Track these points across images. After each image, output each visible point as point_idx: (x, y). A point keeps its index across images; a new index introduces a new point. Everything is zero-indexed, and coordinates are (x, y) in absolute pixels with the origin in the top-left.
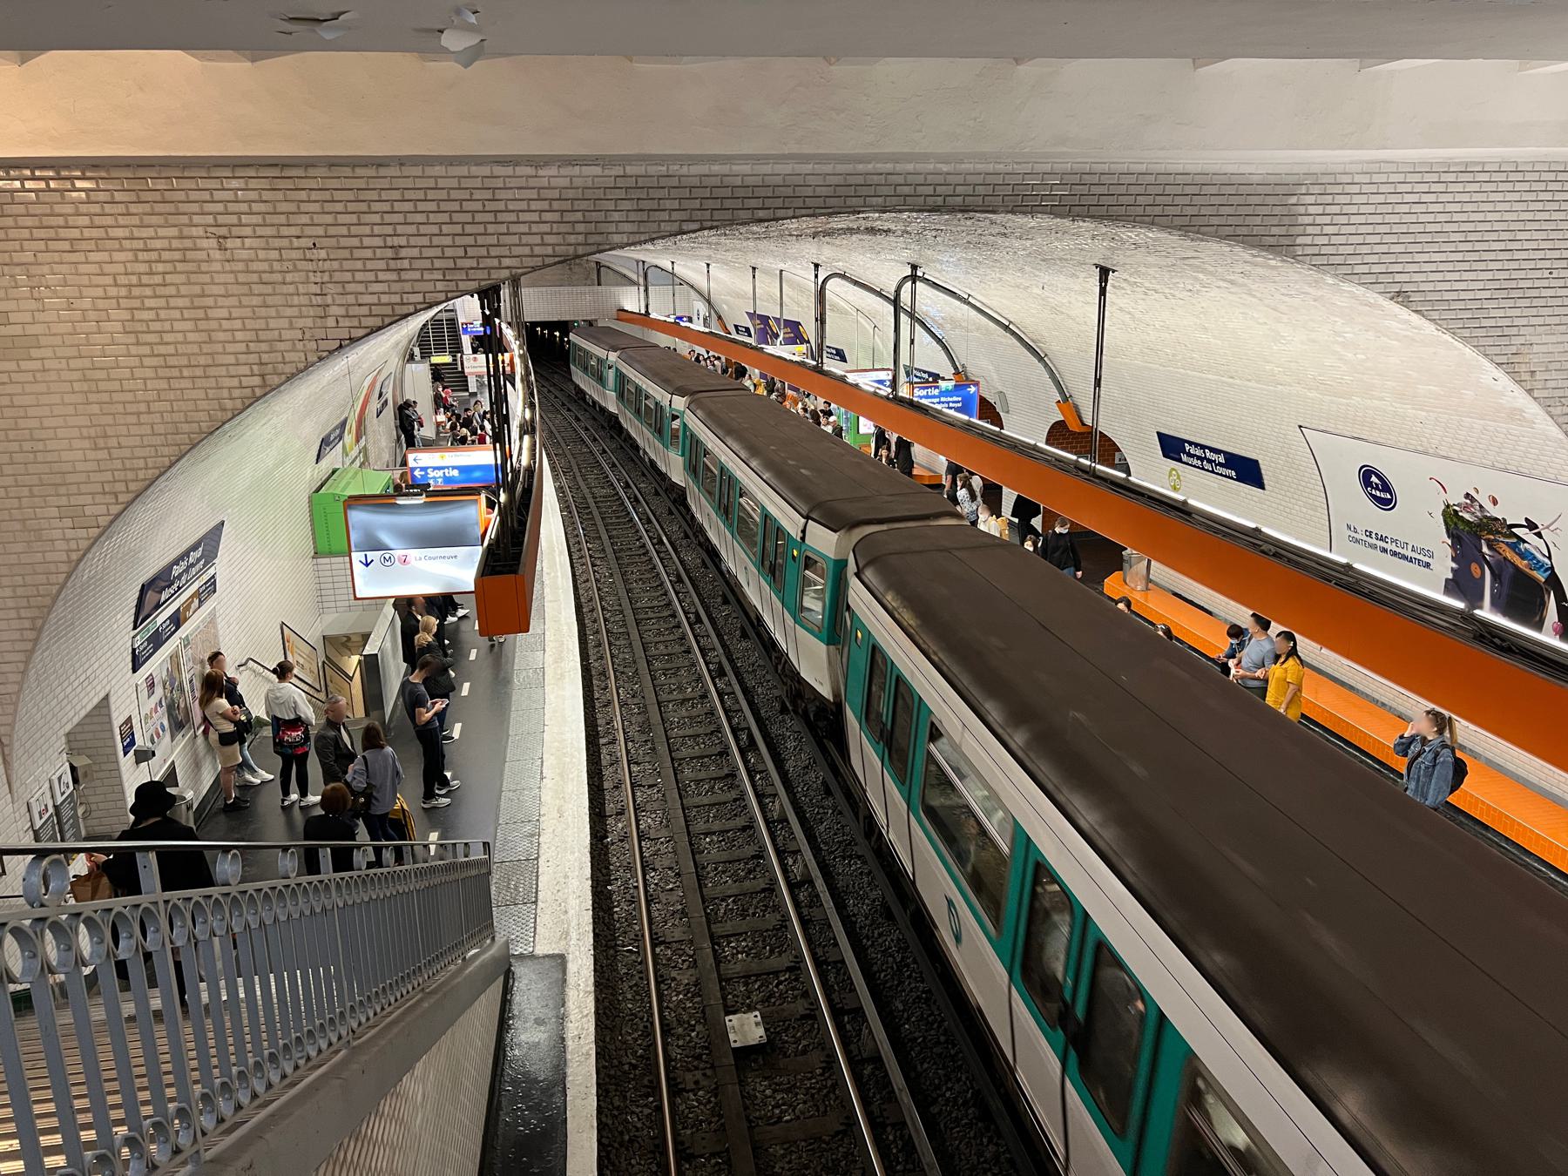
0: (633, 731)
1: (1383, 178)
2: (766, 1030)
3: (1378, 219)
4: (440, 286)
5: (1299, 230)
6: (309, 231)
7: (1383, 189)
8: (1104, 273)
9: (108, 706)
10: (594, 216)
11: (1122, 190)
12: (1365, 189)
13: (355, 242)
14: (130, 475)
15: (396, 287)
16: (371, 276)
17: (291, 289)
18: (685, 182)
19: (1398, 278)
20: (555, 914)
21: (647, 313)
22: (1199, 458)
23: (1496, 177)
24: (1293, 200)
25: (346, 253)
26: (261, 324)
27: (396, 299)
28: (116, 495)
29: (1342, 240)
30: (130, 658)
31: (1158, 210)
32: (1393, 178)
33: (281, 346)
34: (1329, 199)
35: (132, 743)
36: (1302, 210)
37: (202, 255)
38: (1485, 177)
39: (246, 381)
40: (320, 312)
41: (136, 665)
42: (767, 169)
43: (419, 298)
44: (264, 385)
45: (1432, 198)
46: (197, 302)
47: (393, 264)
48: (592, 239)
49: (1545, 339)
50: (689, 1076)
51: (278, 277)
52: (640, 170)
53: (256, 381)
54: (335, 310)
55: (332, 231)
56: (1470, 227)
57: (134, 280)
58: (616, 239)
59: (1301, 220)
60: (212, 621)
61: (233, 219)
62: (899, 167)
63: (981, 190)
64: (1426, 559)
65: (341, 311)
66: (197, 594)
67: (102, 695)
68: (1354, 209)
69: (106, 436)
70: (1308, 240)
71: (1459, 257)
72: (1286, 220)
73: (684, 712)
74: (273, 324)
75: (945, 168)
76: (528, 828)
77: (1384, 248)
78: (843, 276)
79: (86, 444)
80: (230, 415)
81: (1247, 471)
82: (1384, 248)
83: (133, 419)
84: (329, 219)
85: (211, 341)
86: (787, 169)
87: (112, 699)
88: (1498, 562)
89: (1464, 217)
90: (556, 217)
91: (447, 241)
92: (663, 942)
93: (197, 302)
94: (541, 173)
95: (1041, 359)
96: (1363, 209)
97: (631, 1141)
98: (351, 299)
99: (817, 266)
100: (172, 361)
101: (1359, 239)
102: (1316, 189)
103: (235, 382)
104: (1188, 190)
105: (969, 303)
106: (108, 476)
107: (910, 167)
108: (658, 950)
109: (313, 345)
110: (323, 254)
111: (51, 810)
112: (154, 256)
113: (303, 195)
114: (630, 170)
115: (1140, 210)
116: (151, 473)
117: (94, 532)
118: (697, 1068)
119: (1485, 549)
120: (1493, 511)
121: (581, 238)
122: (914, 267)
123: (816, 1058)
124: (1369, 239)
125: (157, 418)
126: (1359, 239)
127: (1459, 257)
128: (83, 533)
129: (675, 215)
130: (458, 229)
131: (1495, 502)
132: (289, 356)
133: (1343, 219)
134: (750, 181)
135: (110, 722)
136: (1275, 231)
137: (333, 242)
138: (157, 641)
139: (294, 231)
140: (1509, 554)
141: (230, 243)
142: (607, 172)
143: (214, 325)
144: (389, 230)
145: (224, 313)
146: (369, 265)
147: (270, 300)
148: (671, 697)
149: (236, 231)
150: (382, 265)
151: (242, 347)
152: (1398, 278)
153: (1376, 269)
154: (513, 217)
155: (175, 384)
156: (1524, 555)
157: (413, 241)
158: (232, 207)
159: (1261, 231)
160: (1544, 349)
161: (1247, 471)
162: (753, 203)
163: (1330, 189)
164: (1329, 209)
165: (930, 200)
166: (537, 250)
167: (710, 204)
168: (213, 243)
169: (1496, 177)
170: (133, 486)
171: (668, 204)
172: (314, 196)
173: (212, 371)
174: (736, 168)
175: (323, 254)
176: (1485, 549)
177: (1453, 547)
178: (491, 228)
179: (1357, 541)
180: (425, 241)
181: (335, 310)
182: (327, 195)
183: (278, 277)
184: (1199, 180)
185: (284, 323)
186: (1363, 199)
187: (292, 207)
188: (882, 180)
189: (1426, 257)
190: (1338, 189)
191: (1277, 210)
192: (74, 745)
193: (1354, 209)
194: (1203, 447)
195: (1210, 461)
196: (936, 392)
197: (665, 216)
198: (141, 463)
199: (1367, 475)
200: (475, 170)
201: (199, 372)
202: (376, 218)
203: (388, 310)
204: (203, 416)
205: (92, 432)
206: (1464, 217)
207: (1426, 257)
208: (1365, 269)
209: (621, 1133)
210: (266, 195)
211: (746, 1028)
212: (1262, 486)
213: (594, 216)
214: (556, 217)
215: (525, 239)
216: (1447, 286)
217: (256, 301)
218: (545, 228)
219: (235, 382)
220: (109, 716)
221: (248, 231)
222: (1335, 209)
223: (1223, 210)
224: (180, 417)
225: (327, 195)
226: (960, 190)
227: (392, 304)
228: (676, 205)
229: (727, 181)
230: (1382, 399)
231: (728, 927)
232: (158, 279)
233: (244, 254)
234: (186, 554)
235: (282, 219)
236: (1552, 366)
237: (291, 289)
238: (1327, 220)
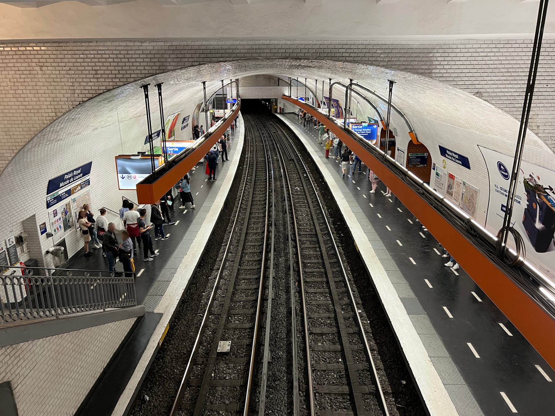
0: (234, 242)
1: (471, 46)
2: (231, 349)
3: (468, 63)
4: (111, 84)
5: (434, 67)
6: (68, 64)
7: (470, 50)
8: (391, 83)
9: (35, 219)
10: (162, 60)
11: (360, 51)
12: (463, 50)
13: (83, 68)
14: (17, 144)
15: (97, 84)
16: (88, 80)
17: (63, 84)
18: (193, 47)
19: (477, 86)
20: (168, 299)
21: (291, 96)
22: (451, 156)
23: (522, 46)
24: (431, 55)
25: (80, 72)
26: (54, 95)
27: (97, 88)
28: (13, 150)
29: (452, 71)
30: (46, 204)
31: (374, 59)
32: (475, 46)
33: (61, 103)
34: (446, 55)
35: (46, 231)
36: (435, 59)
37: (35, 72)
38: (517, 46)
39: (51, 114)
40: (72, 92)
41: (49, 205)
42: (223, 43)
43: (104, 88)
44: (56, 116)
45: (492, 54)
46: (35, 88)
47: (95, 76)
48: (161, 68)
49: (544, 113)
50: (201, 359)
51: (59, 80)
52: (178, 44)
53: (54, 114)
54: (77, 91)
55: (75, 64)
56: (510, 66)
57: (15, 80)
58: (170, 68)
59: (434, 63)
60: (88, 194)
61: (44, 60)
62: (272, 42)
63: (304, 51)
64: (519, 200)
65: (79, 92)
66: (80, 185)
67: (32, 215)
68: (458, 59)
69: (9, 131)
70: (437, 71)
71: (505, 78)
72: (428, 63)
73: (254, 237)
74: (58, 95)
75: (289, 43)
76: (173, 271)
77: (471, 75)
78: (339, 83)
79: (4, 133)
80: (46, 125)
81: (465, 162)
82: (471, 75)
83: (17, 126)
84: (74, 60)
85: (39, 101)
86: (230, 43)
87: (37, 216)
88: (541, 203)
89: (507, 62)
90: (149, 60)
91: (113, 68)
92: (213, 314)
93: (35, 88)
94: (143, 44)
95: (402, 116)
96: (462, 59)
97: (173, 378)
98: (82, 88)
99: (330, 79)
100: (28, 107)
101: (460, 71)
102: (441, 51)
103: (47, 115)
104: (387, 51)
105: (375, 94)
106: (10, 144)
107: (276, 42)
108: (210, 316)
109: (71, 103)
110: (73, 72)
111: (5, 249)
112: (21, 72)
113: (66, 52)
114: (174, 43)
115: (366, 59)
116: (23, 144)
117: (7, 162)
118: (205, 357)
119: (537, 197)
120: (539, 183)
121: (157, 68)
122: (351, 80)
123: (245, 359)
124: (464, 71)
125: (24, 126)
126: (460, 71)
127: (505, 78)
128: (4, 162)
129: (190, 60)
130: (116, 64)
131: (539, 179)
132: (64, 107)
133: (453, 63)
134: (216, 47)
135: (36, 224)
136: (423, 67)
137: (75, 68)
138: (59, 199)
139: (63, 64)
140: (545, 200)
141: (44, 68)
142: (166, 44)
143: (40, 95)
144: (93, 64)
145: (43, 91)
146: (88, 76)
147: (57, 88)
148: (252, 231)
149: (45, 64)
150: (91, 76)
151: (49, 103)
152: (477, 86)
153: (467, 83)
154: (134, 60)
155: (29, 115)
156: (549, 201)
157: (102, 68)
158: (44, 56)
159: (417, 67)
160: (544, 117)
161: (465, 162)
162: (218, 55)
163: (447, 51)
164: (446, 59)
165: (284, 55)
166: (143, 72)
167: (202, 56)
168: (38, 68)
169: (522, 46)
170: (18, 148)
171: (187, 56)
172: (70, 52)
173: (40, 111)
174: (212, 43)
175: (73, 72)
176: (537, 197)
177: (527, 196)
178: (127, 64)
179: (498, 191)
180: (105, 68)
181: (77, 91)
182: (73, 52)
183: (59, 80)
184: (391, 47)
185: (62, 95)
186: (462, 54)
187: (62, 56)
188: (265, 47)
189: (490, 78)
190: (451, 50)
191: (424, 59)
192: (26, 230)
193: (458, 59)
194: (452, 152)
195: (454, 157)
196: (361, 127)
197: (186, 60)
198: (20, 140)
199: (500, 165)
200: (121, 44)
201: (36, 111)
202: (89, 60)
203: (94, 92)
204: (37, 126)
205: (5, 130)
206: (507, 62)
207: (490, 78)
208: (462, 83)
209: (172, 375)
210: (54, 52)
211: (224, 346)
212: (469, 168)
213: (162, 60)
214: (149, 60)
215: (139, 68)
216: (499, 90)
217: (52, 88)
218: (145, 64)
219: (47, 115)
220: (35, 221)
221: (49, 64)
222: (450, 59)
223: (402, 59)
224: (30, 126)
225: (73, 52)
226: (295, 51)
227: (96, 90)
228: (190, 56)
229: (208, 47)
230: (496, 135)
231: (236, 311)
232: (22, 80)
233: (48, 72)
234: (73, 171)
235: (60, 60)
236: (547, 124)
237: (63, 84)
238: (446, 63)
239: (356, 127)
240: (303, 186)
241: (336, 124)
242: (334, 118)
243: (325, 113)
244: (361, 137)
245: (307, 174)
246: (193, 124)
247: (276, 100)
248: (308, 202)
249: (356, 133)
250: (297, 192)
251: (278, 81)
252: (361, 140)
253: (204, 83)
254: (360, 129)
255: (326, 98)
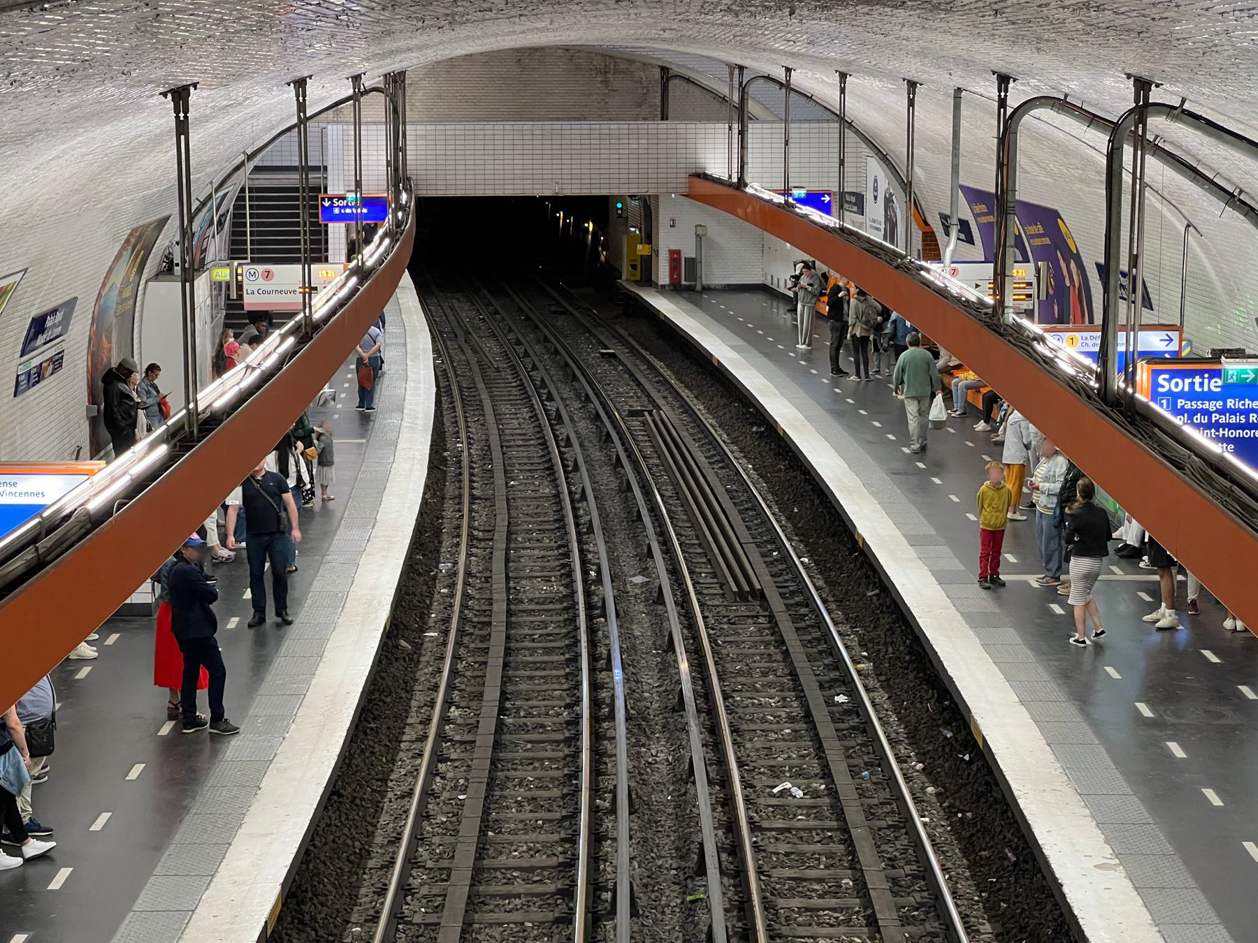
21: (742, 183)
78: (1062, 104)
99: (1004, 80)
122: (1142, 85)
196: (1215, 385)
239: (1183, 385)
240: (826, 774)
241: (1048, 362)
242: (1034, 327)
243: (972, 295)
244: (1216, 448)
245: (852, 692)
246: (94, 353)
247: (648, 207)
248: (862, 889)
249: (1177, 421)
250: (783, 810)
251: (660, 90)
252: (1219, 467)
253: (180, 95)
254: (1210, 396)
255: (974, 196)
